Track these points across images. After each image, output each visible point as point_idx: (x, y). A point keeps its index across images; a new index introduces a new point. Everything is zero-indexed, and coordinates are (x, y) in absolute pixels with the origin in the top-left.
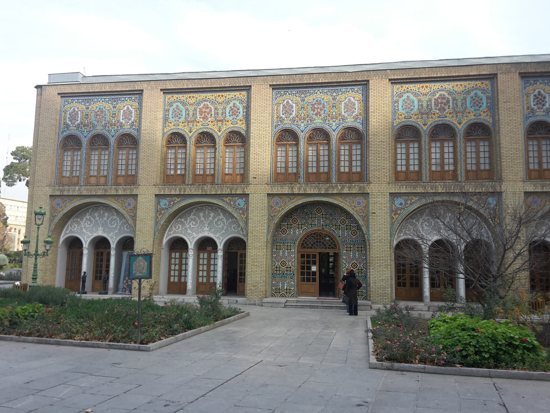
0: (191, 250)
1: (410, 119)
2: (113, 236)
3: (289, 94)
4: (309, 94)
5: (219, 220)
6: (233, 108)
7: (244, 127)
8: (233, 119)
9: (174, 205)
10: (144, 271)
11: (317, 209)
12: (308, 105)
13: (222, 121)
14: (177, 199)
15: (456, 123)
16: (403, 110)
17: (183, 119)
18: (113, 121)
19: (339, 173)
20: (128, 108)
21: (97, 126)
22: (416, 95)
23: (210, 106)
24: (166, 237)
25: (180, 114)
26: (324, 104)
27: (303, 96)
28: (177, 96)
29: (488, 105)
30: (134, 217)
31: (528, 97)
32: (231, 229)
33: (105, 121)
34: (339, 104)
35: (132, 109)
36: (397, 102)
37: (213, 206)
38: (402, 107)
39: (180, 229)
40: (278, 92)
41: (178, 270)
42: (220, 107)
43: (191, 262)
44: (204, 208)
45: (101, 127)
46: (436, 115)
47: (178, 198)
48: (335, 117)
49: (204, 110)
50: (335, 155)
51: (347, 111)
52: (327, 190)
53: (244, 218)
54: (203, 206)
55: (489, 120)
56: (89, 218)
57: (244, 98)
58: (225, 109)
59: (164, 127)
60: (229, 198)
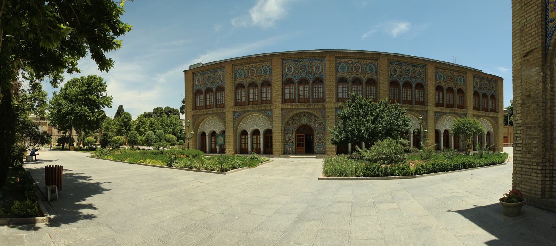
4: (299, 62)
13: (260, 76)
15: (363, 77)
16: (341, 70)
17: (243, 77)
19: (313, 99)
22: (346, 64)
27: (296, 63)
42: (259, 70)
46: (355, 74)
49: (252, 71)
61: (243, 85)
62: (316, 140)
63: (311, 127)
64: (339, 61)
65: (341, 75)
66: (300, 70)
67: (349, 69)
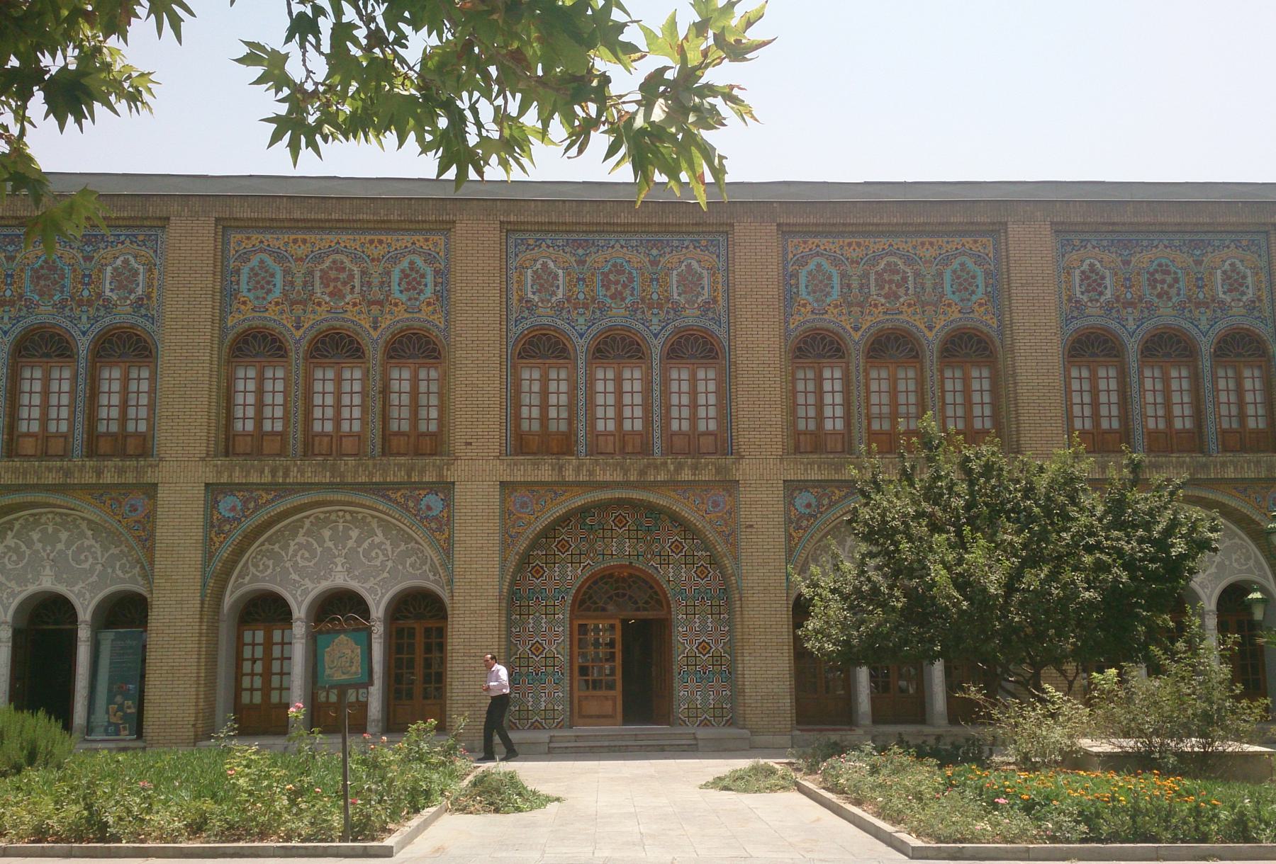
0: (299, 623)
1: (826, 316)
2: (84, 591)
3: (548, 247)
4: (593, 249)
5: (372, 546)
6: (408, 272)
8: (410, 299)
9: (257, 508)
10: (354, 669)
11: (616, 517)
12: (593, 275)
13: (380, 303)
14: (264, 495)
15: (922, 327)
16: (809, 294)
17: (277, 294)
18: (86, 293)
19: (670, 436)
20: (126, 262)
21: (38, 305)
22: (835, 262)
23: (348, 264)
24: (232, 592)
25: (268, 283)
26: (630, 273)
27: (581, 251)
28: (260, 237)
29: (989, 289)
30: (146, 540)
31: (1068, 273)
32: (405, 567)
33: (62, 292)
34: (666, 275)
35: (136, 266)
36: (795, 275)
37: (358, 513)
39: (269, 571)
40: (522, 240)
41: (261, 675)
42: (376, 271)
43: (298, 652)
44: (333, 517)
45: (50, 308)
46: (880, 308)
47: (267, 491)
48: (658, 304)
49: (333, 274)
50: (658, 393)
51: (685, 292)
52: (642, 472)
53: (442, 542)
54: (330, 512)
55: (990, 322)
56: (13, 545)
57: (438, 250)
58: (389, 273)
60: (403, 491)
61: (274, 340)
62: (681, 648)
63: (657, 582)
64: (796, 246)
65: (810, 317)
66: (602, 292)
67: (849, 286)
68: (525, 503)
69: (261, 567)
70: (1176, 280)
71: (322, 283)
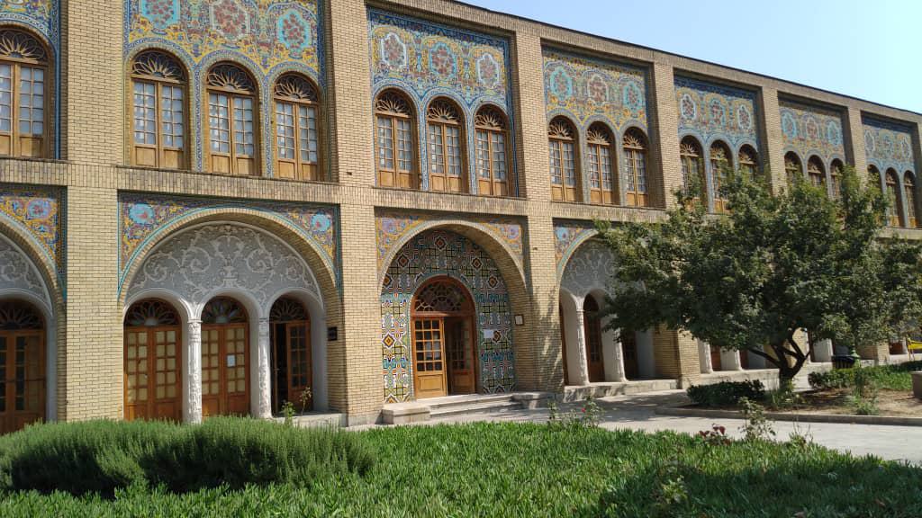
6: (289, 22)
7: (315, 66)
12: (426, 52)
13: (267, 45)
15: (614, 122)
17: (174, 21)
26: (450, 56)
37: (243, 227)
38: (555, 85)
39: (164, 277)
42: (263, 17)
43: (195, 352)
44: (222, 230)
52: (471, 205)
58: (274, 21)
59: (126, 33)
63: (465, 289)
66: (433, 67)
68: (391, 225)
69: (156, 273)
70: (722, 113)
71: (216, 18)
